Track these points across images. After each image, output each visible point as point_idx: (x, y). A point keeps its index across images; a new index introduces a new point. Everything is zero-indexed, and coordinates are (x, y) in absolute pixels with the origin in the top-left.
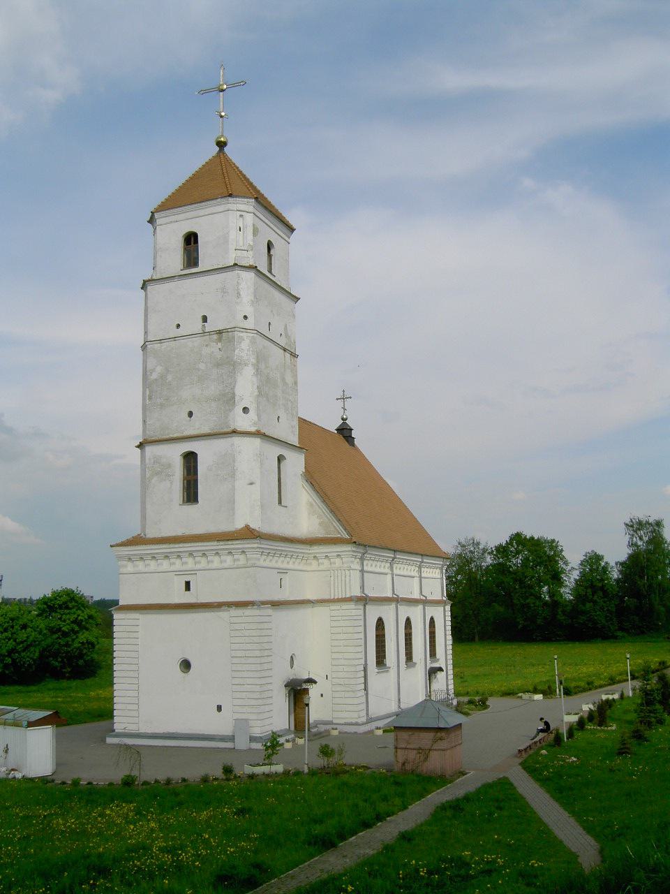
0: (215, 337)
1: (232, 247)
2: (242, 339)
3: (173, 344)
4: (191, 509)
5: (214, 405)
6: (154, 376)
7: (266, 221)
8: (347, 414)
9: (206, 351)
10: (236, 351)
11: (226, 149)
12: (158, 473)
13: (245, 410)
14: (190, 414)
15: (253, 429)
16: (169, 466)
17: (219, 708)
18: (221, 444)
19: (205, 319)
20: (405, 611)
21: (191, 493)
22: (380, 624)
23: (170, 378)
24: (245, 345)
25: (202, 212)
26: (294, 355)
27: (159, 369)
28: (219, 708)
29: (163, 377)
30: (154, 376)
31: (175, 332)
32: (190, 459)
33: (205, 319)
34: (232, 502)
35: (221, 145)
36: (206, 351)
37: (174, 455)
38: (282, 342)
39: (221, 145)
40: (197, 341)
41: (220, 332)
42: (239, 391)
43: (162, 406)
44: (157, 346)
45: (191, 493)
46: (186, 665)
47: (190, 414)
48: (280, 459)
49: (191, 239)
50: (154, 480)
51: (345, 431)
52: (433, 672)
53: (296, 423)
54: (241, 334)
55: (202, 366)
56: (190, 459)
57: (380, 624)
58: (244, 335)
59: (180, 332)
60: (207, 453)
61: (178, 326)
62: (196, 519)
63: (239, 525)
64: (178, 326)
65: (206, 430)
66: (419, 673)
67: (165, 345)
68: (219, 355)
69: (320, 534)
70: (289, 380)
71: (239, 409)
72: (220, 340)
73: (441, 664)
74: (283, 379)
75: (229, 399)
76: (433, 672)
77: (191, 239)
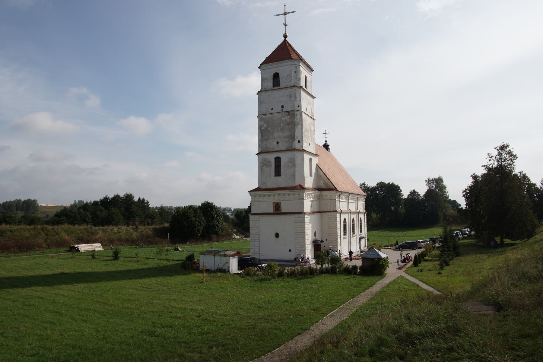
0: (287, 114)
1: (293, 79)
3: (270, 116)
4: (278, 178)
5: (287, 139)
6: (263, 128)
9: (283, 119)
11: (287, 39)
12: (265, 165)
13: (299, 142)
14: (278, 143)
16: (270, 162)
17: (290, 251)
18: (289, 154)
19: (282, 107)
20: (353, 216)
21: (278, 172)
22: (345, 220)
23: (269, 129)
24: (298, 117)
25: (281, 65)
26: (314, 120)
27: (265, 125)
28: (290, 251)
29: (266, 128)
30: (263, 128)
31: (271, 111)
32: (278, 160)
33: (282, 107)
34: (294, 176)
35: (285, 36)
36: (283, 119)
37: (271, 157)
38: (310, 115)
39: (285, 36)
40: (280, 115)
41: (289, 112)
43: (267, 139)
44: (264, 116)
45: (278, 172)
46: (277, 235)
47: (278, 143)
48: (311, 160)
49: (276, 76)
50: (264, 167)
52: (360, 239)
53: (314, 146)
55: (282, 125)
56: (278, 160)
57: (345, 220)
58: (298, 113)
59: (273, 111)
60: (285, 158)
61: (272, 109)
62: (281, 182)
63: (297, 184)
64: (272, 109)
65: (284, 149)
66: (355, 240)
67: (267, 116)
68: (289, 120)
70: (313, 130)
71: (296, 141)
72: (289, 115)
73: (363, 236)
74: (311, 129)
75: (292, 137)
76: (360, 239)
77: (276, 76)
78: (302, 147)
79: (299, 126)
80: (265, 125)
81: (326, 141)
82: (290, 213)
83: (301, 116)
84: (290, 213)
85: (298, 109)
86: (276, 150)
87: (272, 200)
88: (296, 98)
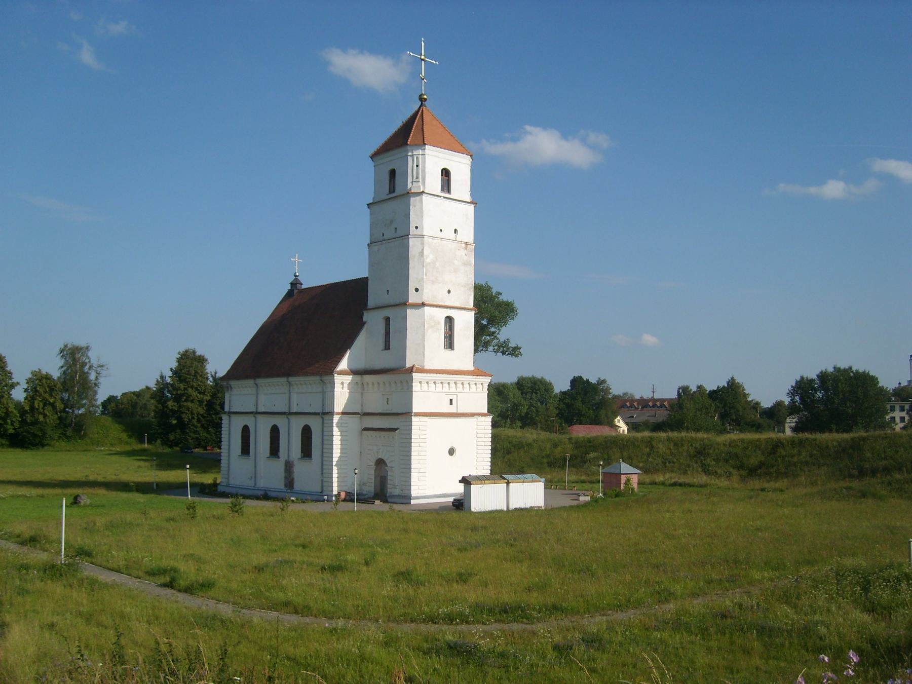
12: (432, 327)
14: (449, 292)
16: (439, 323)
19: (456, 231)
23: (438, 264)
27: (431, 256)
32: (449, 320)
33: (456, 231)
43: (433, 282)
44: (430, 240)
46: (452, 452)
47: (449, 292)
50: (430, 331)
55: (456, 262)
56: (449, 320)
65: (457, 304)
67: (435, 241)
72: (466, 249)
80: (431, 256)
82: (472, 415)
84: (472, 415)
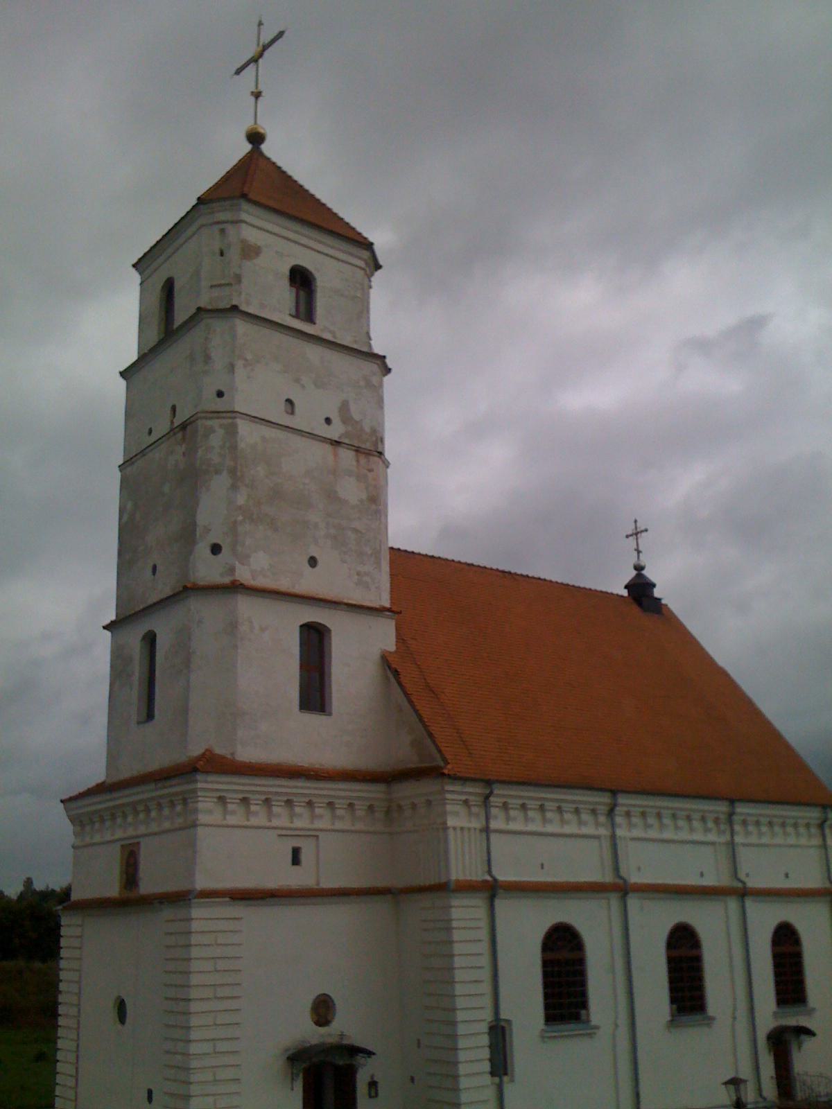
2: (211, 430)
7: (291, 235)
8: (644, 560)
10: (200, 453)
13: (216, 549)
15: (227, 580)
24: (216, 440)
35: (256, 138)
39: (256, 138)
42: (202, 519)
51: (641, 589)
54: (209, 423)
58: (215, 423)
61: (150, 432)
63: (196, 750)
64: (150, 432)
69: (413, 762)
71: (203, 549)
78: (232, 570)
79: (220, 483)
81: (639, 568)
83: (232, 431)
85: (220, 405)
86: (150, 602)
87: (119, 834)
88: (208, 358)
